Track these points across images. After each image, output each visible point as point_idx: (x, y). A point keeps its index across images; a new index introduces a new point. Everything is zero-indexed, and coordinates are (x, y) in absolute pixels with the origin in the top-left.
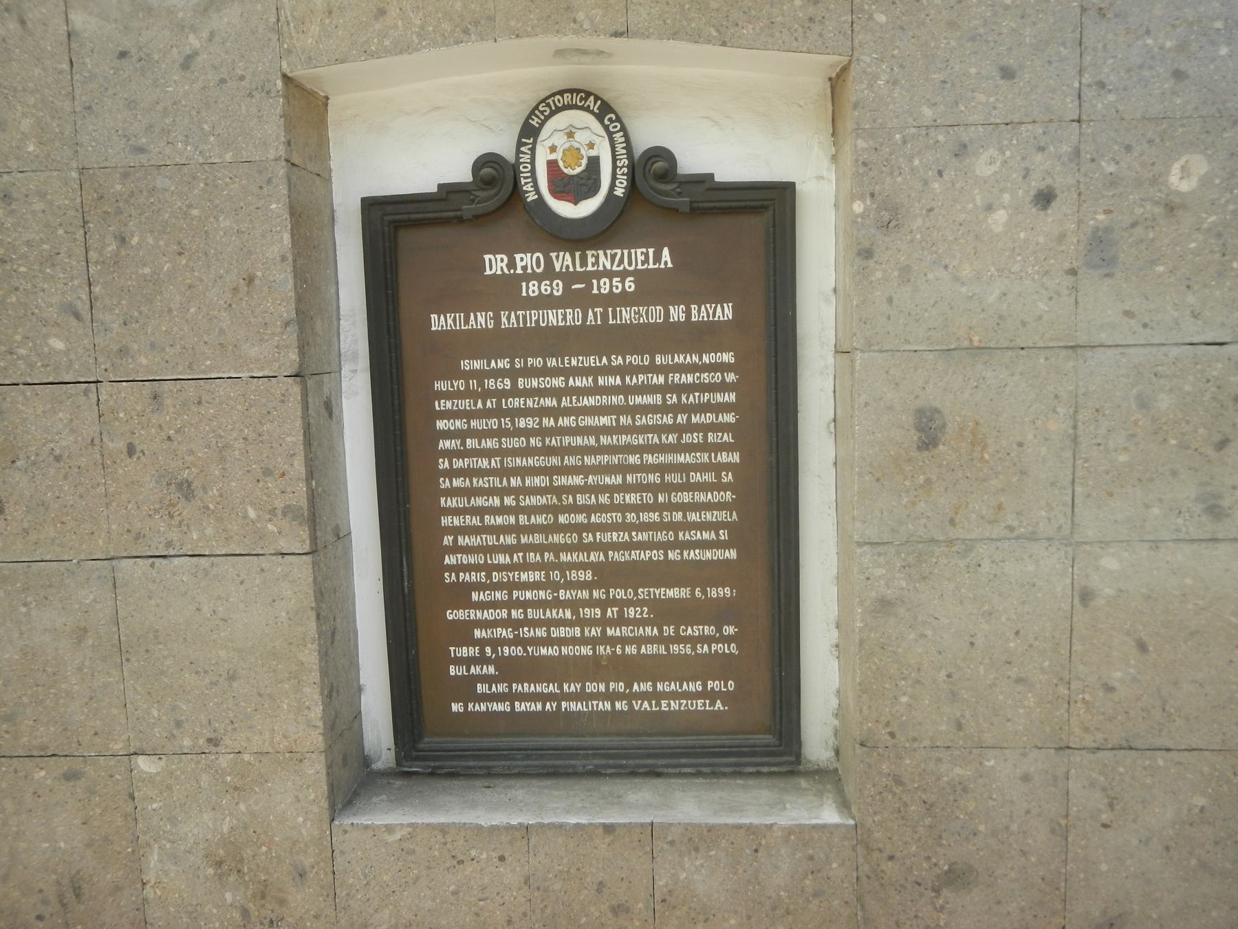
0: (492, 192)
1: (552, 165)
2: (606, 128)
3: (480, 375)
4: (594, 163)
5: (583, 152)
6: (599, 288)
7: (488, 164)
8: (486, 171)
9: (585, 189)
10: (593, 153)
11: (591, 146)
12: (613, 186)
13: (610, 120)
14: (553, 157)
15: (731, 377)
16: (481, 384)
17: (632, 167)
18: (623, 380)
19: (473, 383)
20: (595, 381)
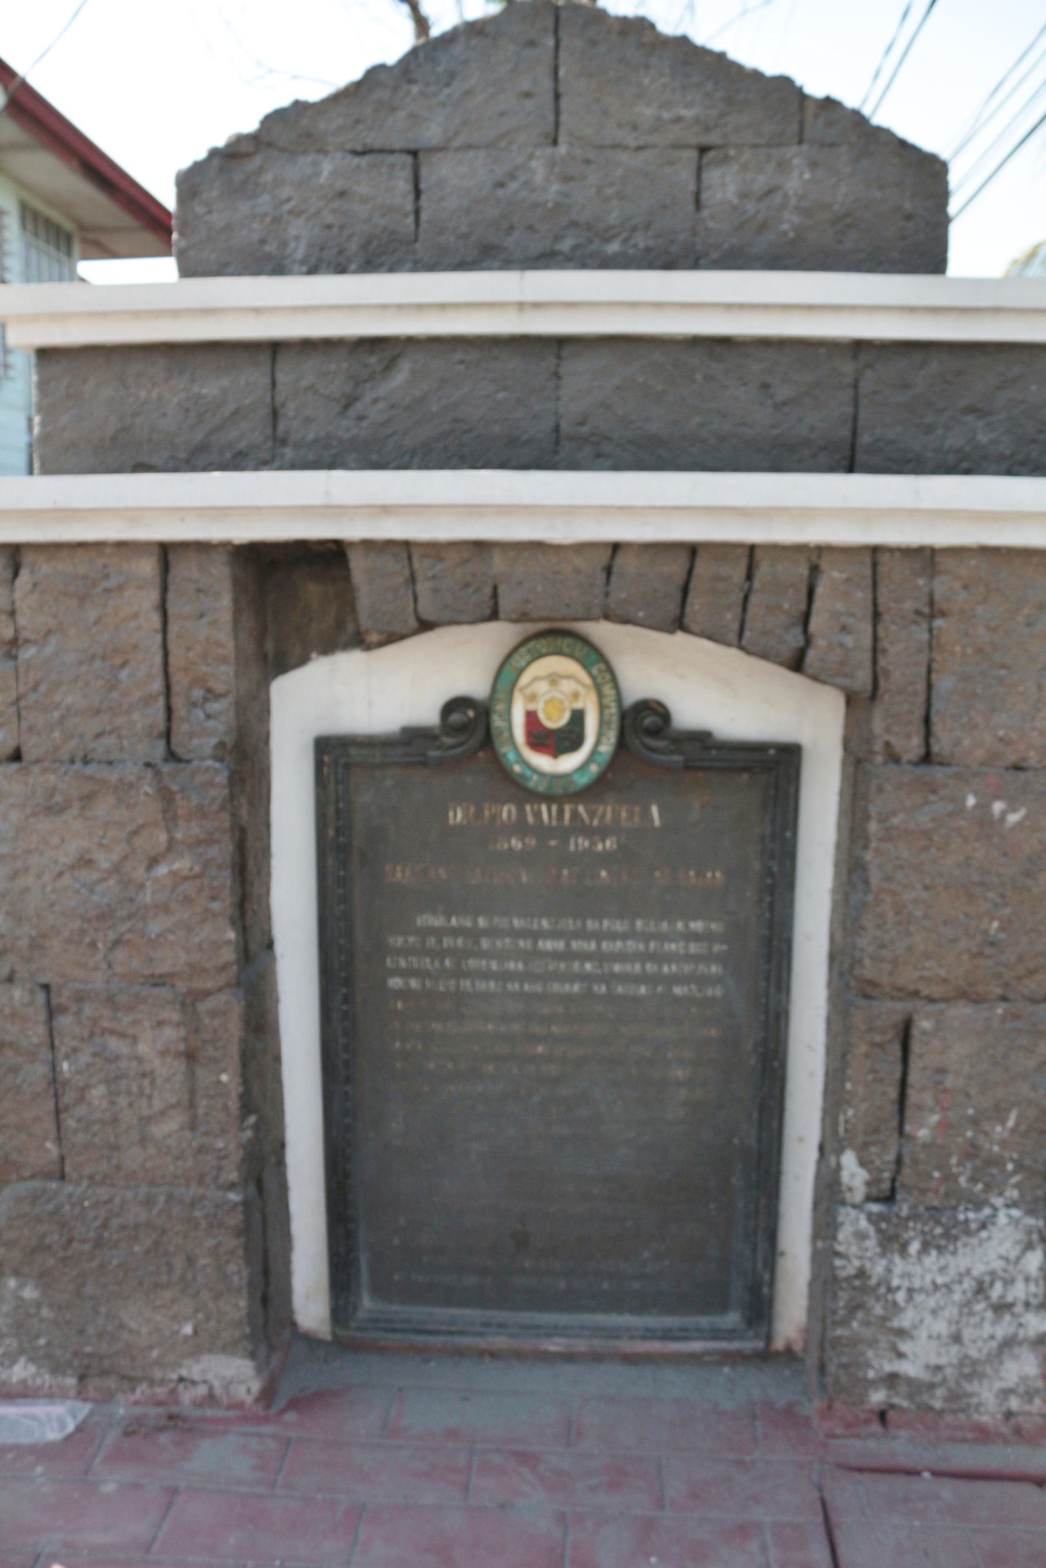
0: (461, 738)
1: (531, 717)
2: (593, 677)
3: (438, 933)
4: (578, 718)
5: (567, 704)
6: (576, 845)
7: (454, 705)
8: (455, 718)
9: (567, 744)
10: (578, 705)
11: (576, 696)
12: (598, 743)
13: (600, 671)
14: (531, 707)
15: (717, 948)
16: (440, 942)
17: (623, 715)
18: (599, 944)
19: (431, 941)
20: (568, 945)
